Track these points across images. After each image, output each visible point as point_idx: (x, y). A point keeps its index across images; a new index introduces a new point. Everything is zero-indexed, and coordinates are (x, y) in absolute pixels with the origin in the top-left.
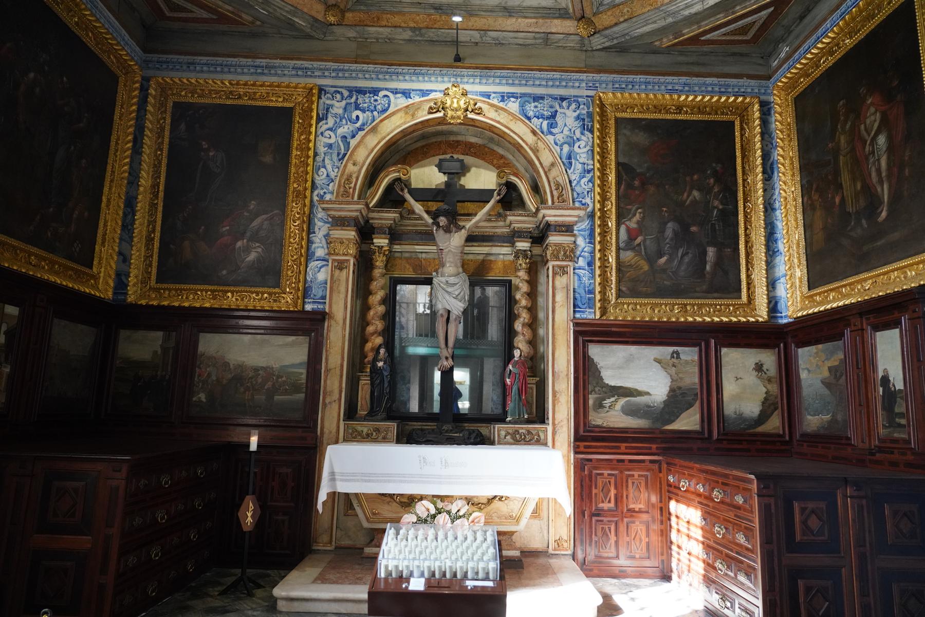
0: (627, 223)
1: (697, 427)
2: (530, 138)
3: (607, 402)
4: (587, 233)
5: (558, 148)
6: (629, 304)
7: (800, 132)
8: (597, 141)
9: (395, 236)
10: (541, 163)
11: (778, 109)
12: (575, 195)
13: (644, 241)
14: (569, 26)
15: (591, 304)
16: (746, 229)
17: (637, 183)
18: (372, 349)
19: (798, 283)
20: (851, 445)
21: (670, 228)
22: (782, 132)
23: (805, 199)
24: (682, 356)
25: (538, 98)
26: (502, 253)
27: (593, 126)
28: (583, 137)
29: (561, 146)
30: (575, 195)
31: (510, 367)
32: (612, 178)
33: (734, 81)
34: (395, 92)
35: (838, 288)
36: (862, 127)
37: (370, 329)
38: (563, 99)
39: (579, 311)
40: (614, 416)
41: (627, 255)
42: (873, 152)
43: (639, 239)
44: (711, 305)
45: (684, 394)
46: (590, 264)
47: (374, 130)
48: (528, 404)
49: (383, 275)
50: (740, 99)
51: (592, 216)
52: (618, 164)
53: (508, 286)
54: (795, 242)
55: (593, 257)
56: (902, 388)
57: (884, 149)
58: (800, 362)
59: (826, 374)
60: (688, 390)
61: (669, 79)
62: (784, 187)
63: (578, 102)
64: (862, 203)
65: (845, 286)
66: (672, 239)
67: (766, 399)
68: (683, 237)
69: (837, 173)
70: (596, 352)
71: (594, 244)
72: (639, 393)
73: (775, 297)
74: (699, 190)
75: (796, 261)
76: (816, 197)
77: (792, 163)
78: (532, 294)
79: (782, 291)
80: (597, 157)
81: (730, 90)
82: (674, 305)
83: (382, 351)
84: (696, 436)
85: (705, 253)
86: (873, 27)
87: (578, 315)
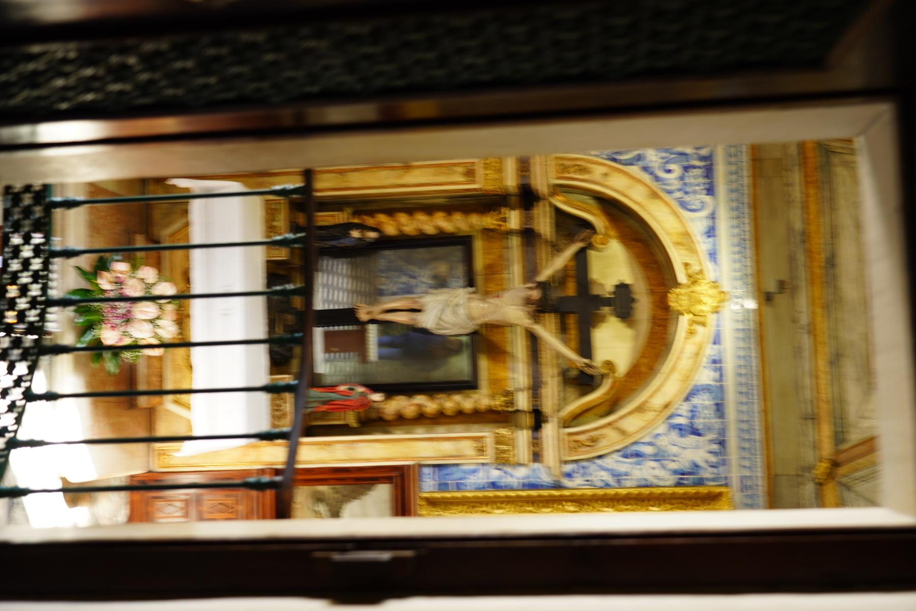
2: (658, 401)
4: (533, 480)
9: (528, 235)
10: (622, 417)
14: (827, 449)
15: (443, 487)
18: (380, 223)
25: (719, 408)
26: (518, 375)
31: (361, 389)
34: (713, 216)
37: (403, 218)
38: (722, 443)
46: (494, 485)
47: (654, 195)
48: (325, 415)
49: (471, 226)
51: (558, 486)
53: (469, 385)
78: (461, 417)
80: (635, 491)
83: (372, 235)
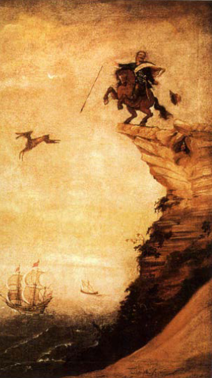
67: (159, 233)
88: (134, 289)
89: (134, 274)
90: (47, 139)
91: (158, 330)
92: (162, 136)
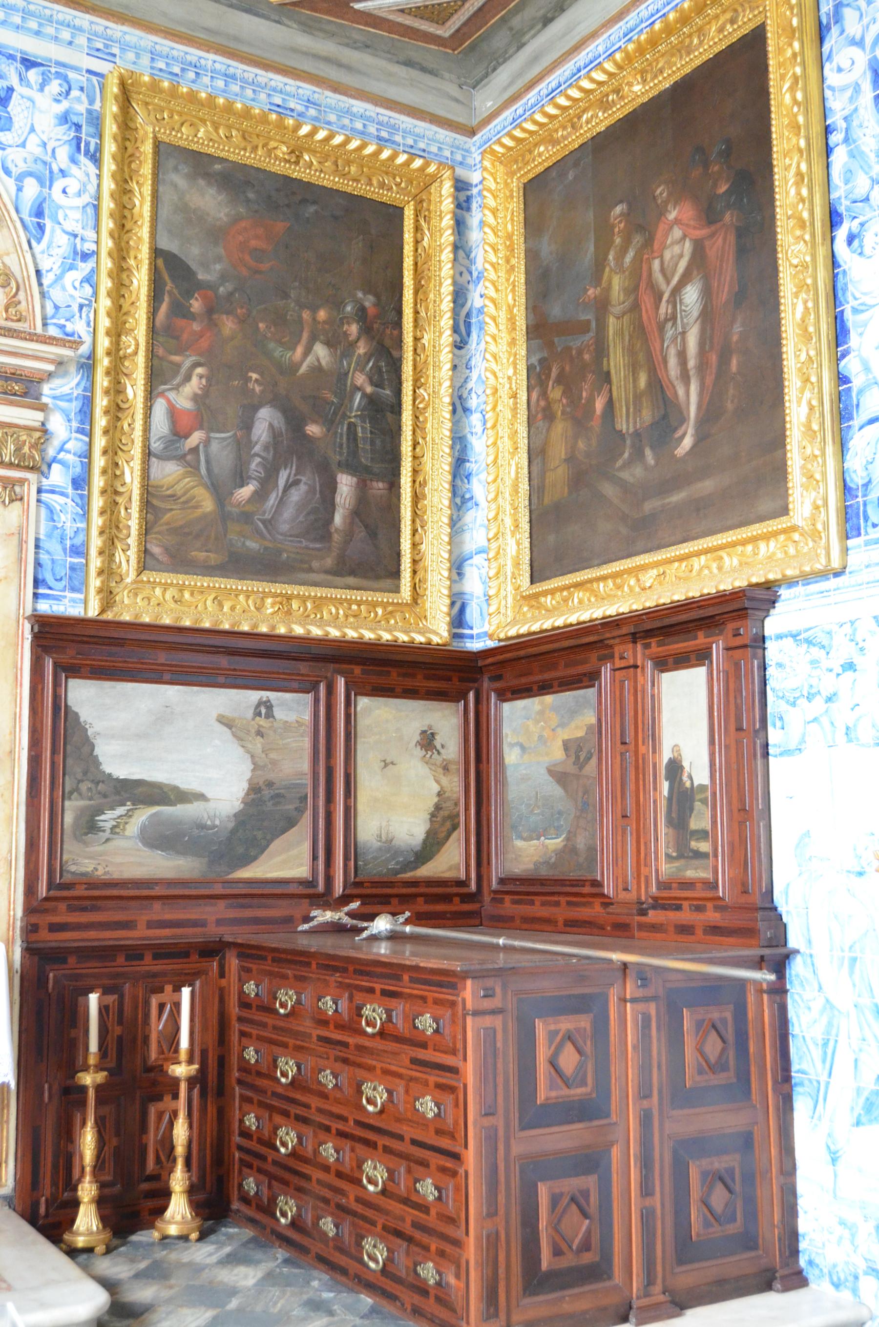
0: (171, 395)
1: (302, 871)
3: (108, 818)
4: (75, 406)
5: (11, 183)
6: (166, 587)
7: (532, 256)
8: (109, 185)
11: (491, 201)
12: (50, 310)
13: (207, 442)
16: (415, 445)
17: (196, 305)
19: (509, 569)
20: (603, 895)
21: (266, 420)
22: (496, 251)
23: (535, 395)
24: (278, 713)
27: (99, 148)
28: (74, 170)
29: (20, 179)
30: (50, 310)
32: (140, 280)
33: (405, 121)
35: (590, 581)
36: (656, 264)
38: (29, 63)
39: (46, 596)
40: (122, 852)
41: (168, 472)
42: (674, 318)
43: (196, 438)
44: (341, 601)
45: (278, 797)
46: (80, 482)
50: (418, 163)
51: (88, 365)
52: (156, 252)
54: (509, 482)
55: (88, 467)
56: (706, 781)
57: (695, 314)
58: (506, 730)
59: (558, 754)
60: (287, 788)
61: (278, 80)
62: (493, 365)
63: (65, 79)
64: (647, 416)
65: (604, 578)
66: (266, 448)
67: (438, 807)
68: (292, 445)
69: (601, 349)
70: (85, 696)
71: (90, 435)
72: (182, 796)
73: (461, 594)
74: (328, 344)
75: (509, 522)
76: (556, 393)
77: (512, 320)
79: (473, 584)
80: (107, 224)
81: (398, 138)
82: (265, 595)
84: (301, 890)
85: (331, 487)
86: (688, 70)
87: (44, 607)
88: (428, 833)
89: (428, 826)
90: (392, 763)
91: (439, 851)
92: (438, 763)
